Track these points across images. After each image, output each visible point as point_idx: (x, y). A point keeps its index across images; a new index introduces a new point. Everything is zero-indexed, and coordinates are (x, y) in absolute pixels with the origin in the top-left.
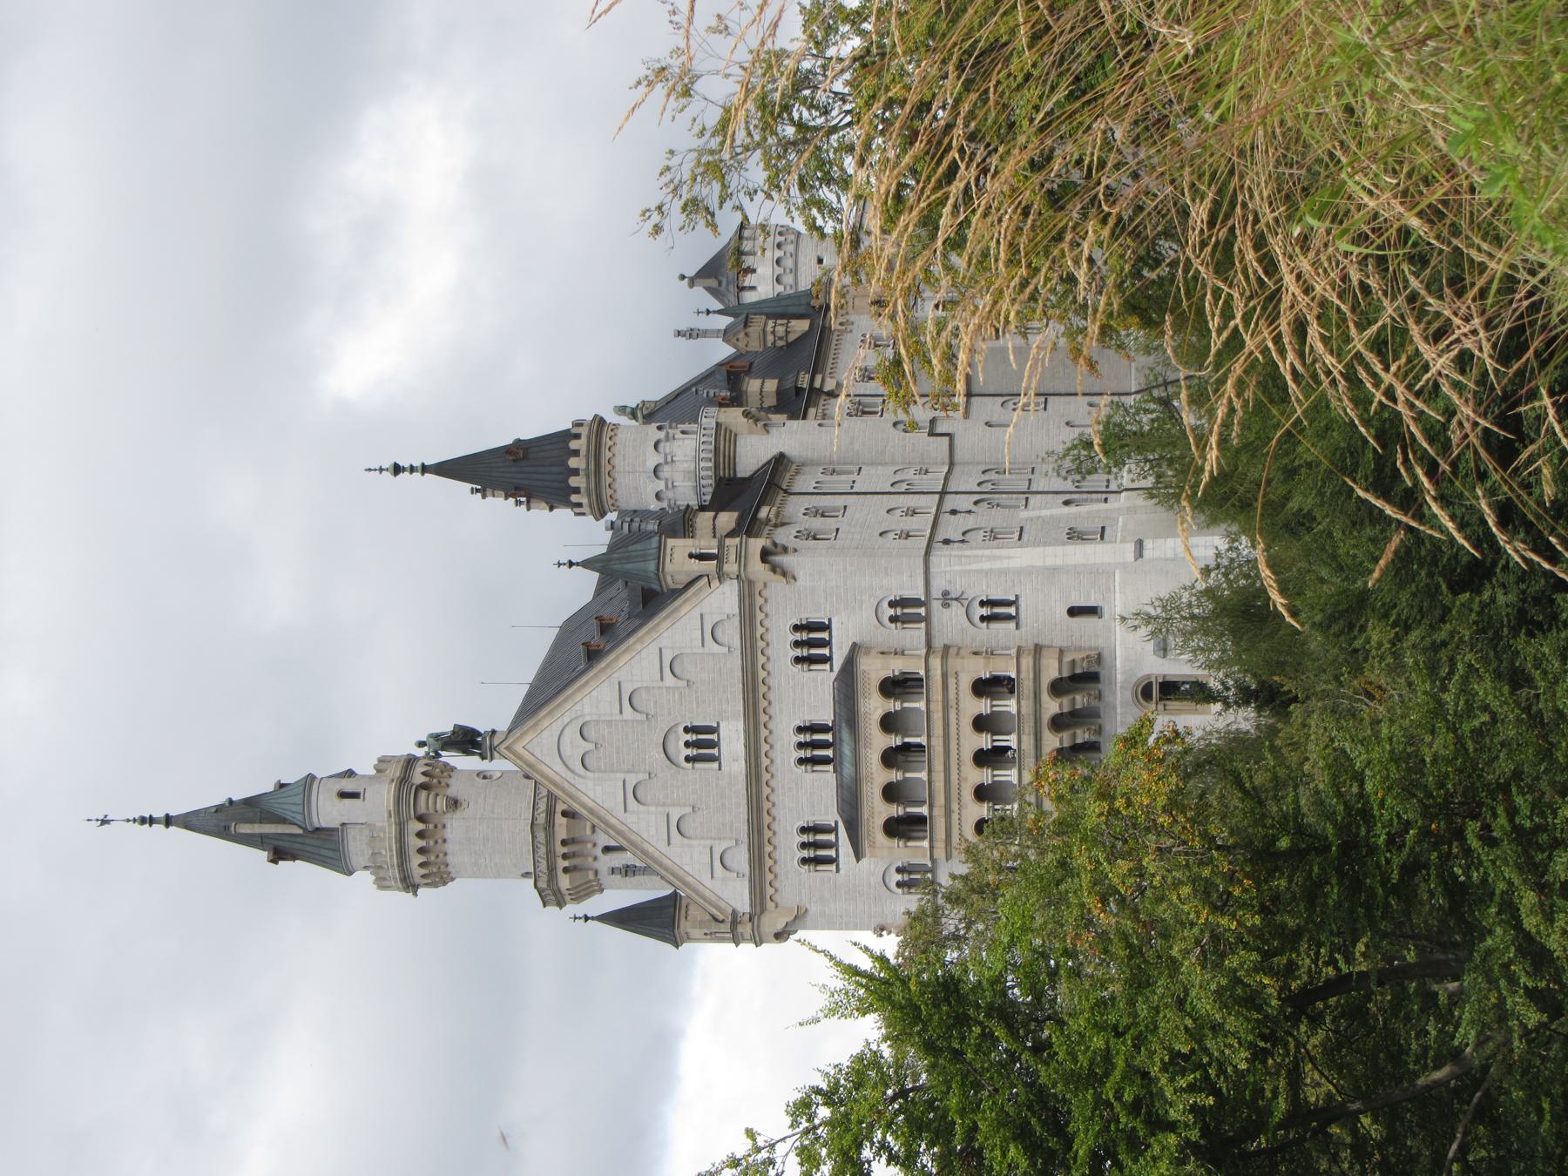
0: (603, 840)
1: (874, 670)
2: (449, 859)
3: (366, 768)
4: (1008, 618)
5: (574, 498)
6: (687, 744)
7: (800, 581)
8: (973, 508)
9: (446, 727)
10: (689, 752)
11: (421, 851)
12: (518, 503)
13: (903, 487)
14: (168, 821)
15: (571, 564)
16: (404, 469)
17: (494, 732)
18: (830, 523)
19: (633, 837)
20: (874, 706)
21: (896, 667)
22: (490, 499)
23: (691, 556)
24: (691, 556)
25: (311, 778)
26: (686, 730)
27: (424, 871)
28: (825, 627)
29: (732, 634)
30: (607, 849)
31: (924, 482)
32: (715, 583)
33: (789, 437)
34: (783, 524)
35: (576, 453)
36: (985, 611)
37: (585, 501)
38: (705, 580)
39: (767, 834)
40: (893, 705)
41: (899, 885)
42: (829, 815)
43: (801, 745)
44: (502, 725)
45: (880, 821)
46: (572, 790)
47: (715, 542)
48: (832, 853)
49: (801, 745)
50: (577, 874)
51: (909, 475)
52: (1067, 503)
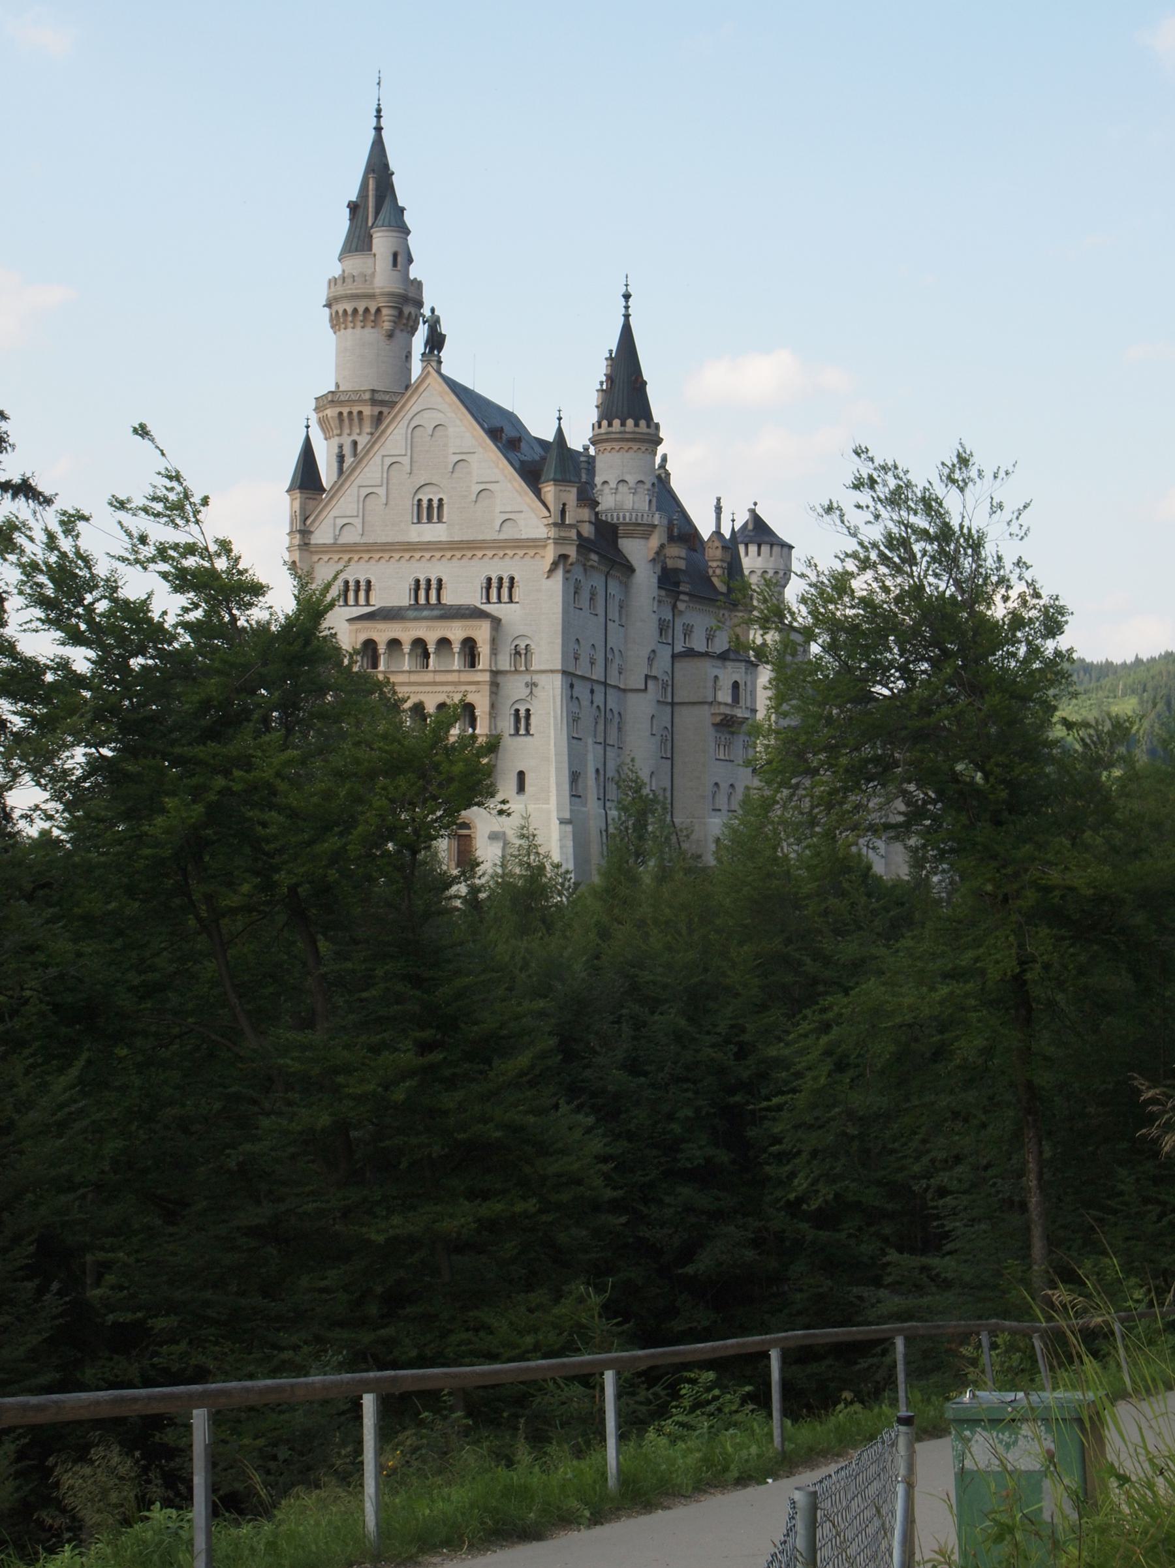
0: (363, 441)
1: (482, 633)
2: (350, 331)
3: (414, 272)
4: (517, 729)
5: (605, 423)
6: (430, 500)
7: (544, 581)
8: (595, 705)
9: (444, 329)
10: (425, 504)
11: (355, 311)
12: (602, 383)
13: (610, 656)
14: (378, 129)
15: (560, 419)
16: (627, 302)
17: (440, 362)
18: (585, 604)
19: (365, 462)
20: (456, 632)
21: (484, 649)
22: (605, 363)
23: (564, 505)
24: (564, 505)
25: (407, 232)
26: (441, 500)
27: (341, 312)
29: (508, 533)
30: (355, 443)
32: (545, 521)
33: (645, 578)
34: (585, 570)
35: (636, 425)
36: (522, 713)
39: (366, 556)
40: (456, 647)
42: (379, 600)
43: (429, 581)
44: (443, 371)
45: (375, 636)
46: (399, 419)
47: (573, 522)
48: (351, 601)
50: (337, 422)
51: (617, 661)
52: (597, 771)
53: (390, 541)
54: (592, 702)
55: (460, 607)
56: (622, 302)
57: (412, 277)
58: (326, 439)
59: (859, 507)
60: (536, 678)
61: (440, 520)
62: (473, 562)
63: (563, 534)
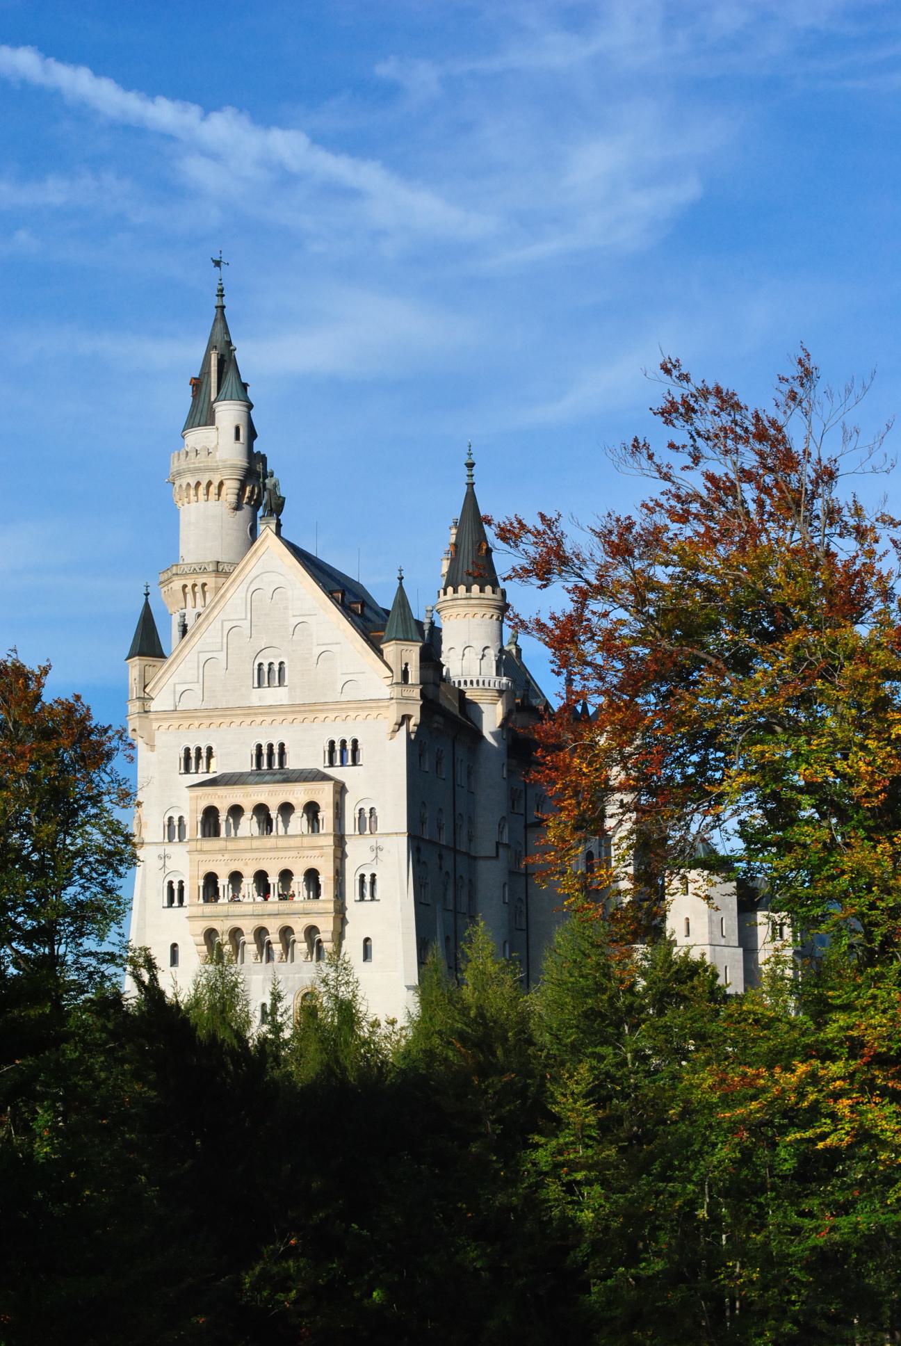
1: (324, 795)
5: (450, 589)
9: (282, 492)
15: (401, 579)
20: (298, 795)
28: (355, 763)
29: (350, 694)
32: (389, 681)
35: (482, 590)
37: (448, 597)
41: (170, 819)
42: (218, 767)
43: (270, 746)
46: (238, 582)
49: (270, 746)
54: (441, 868)
55: (302, 771)
56: (466, 471)
57: (255, 451)
59: (672, 446)
60: (382, 842)
62: (315, 725)
63: (405, 694)
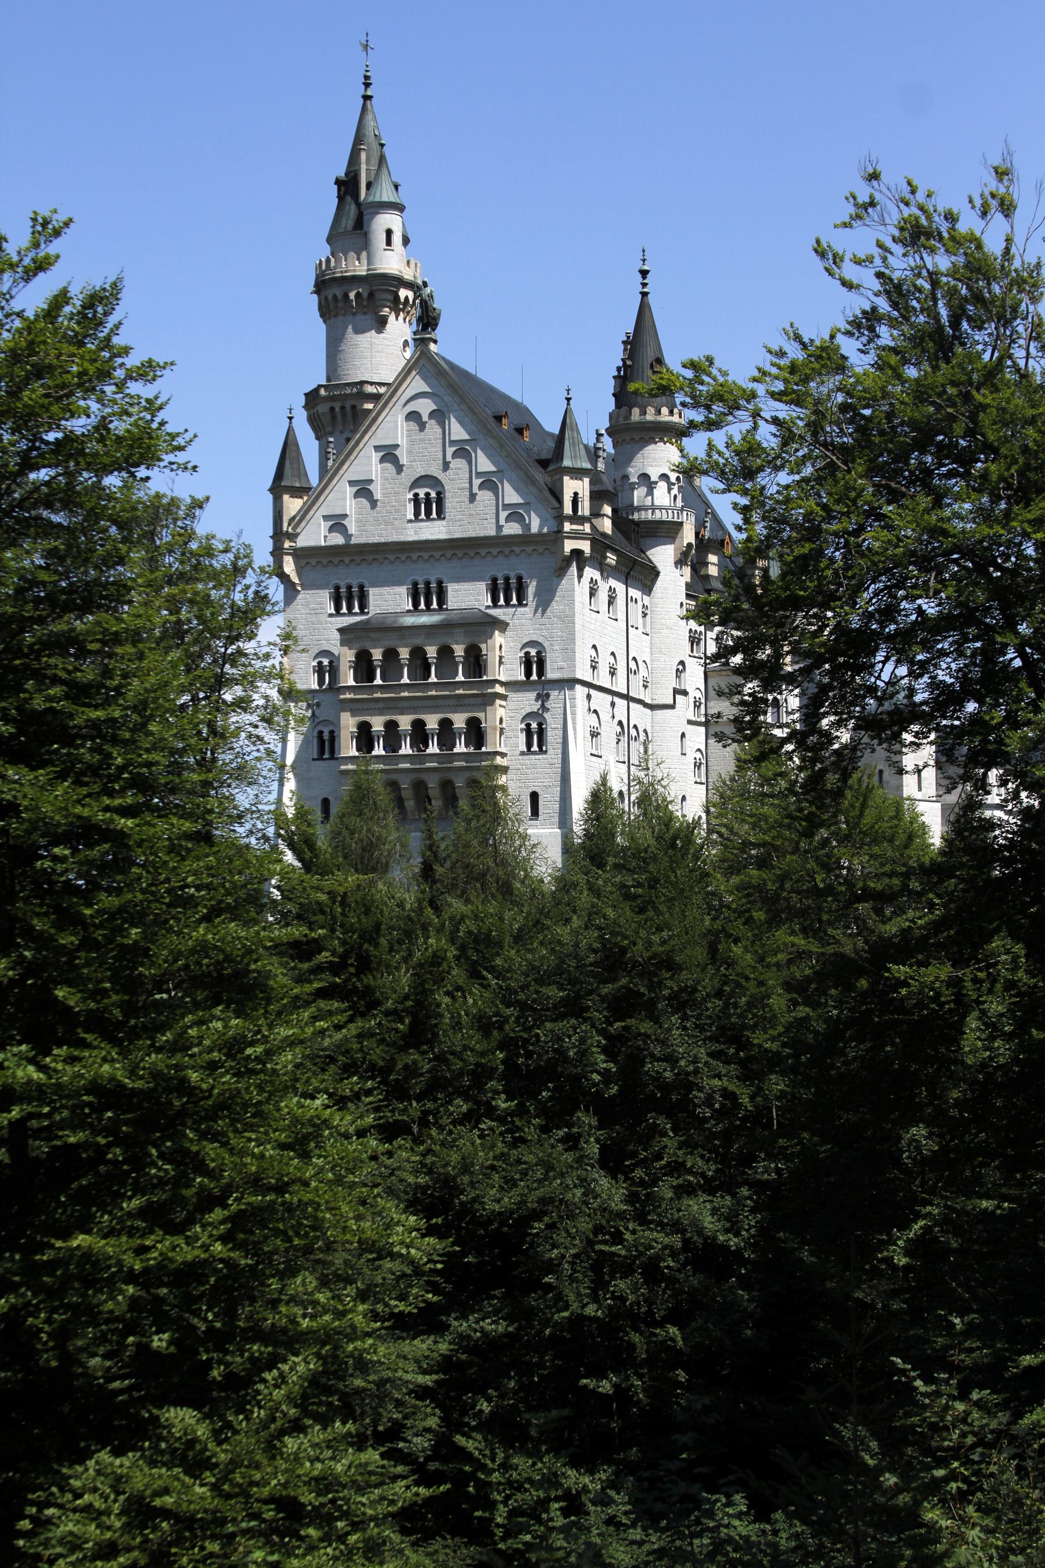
6: (427, 494)
12: (619, 369)
14: (367, 98)
15: (568, 400)
16: (644, 278)
18: (603, 606)
19: (355, 454)
22: (622, 347)
23: (576, 494)
24: (576, 494)
27: (330, 298)
31: (636, 682)
38: (557, 505)
39: (358, 558)
46: (390, 405)
48: (344, 610)
53: (383, 540)
58: (317, 438)
61: (441, 515)
